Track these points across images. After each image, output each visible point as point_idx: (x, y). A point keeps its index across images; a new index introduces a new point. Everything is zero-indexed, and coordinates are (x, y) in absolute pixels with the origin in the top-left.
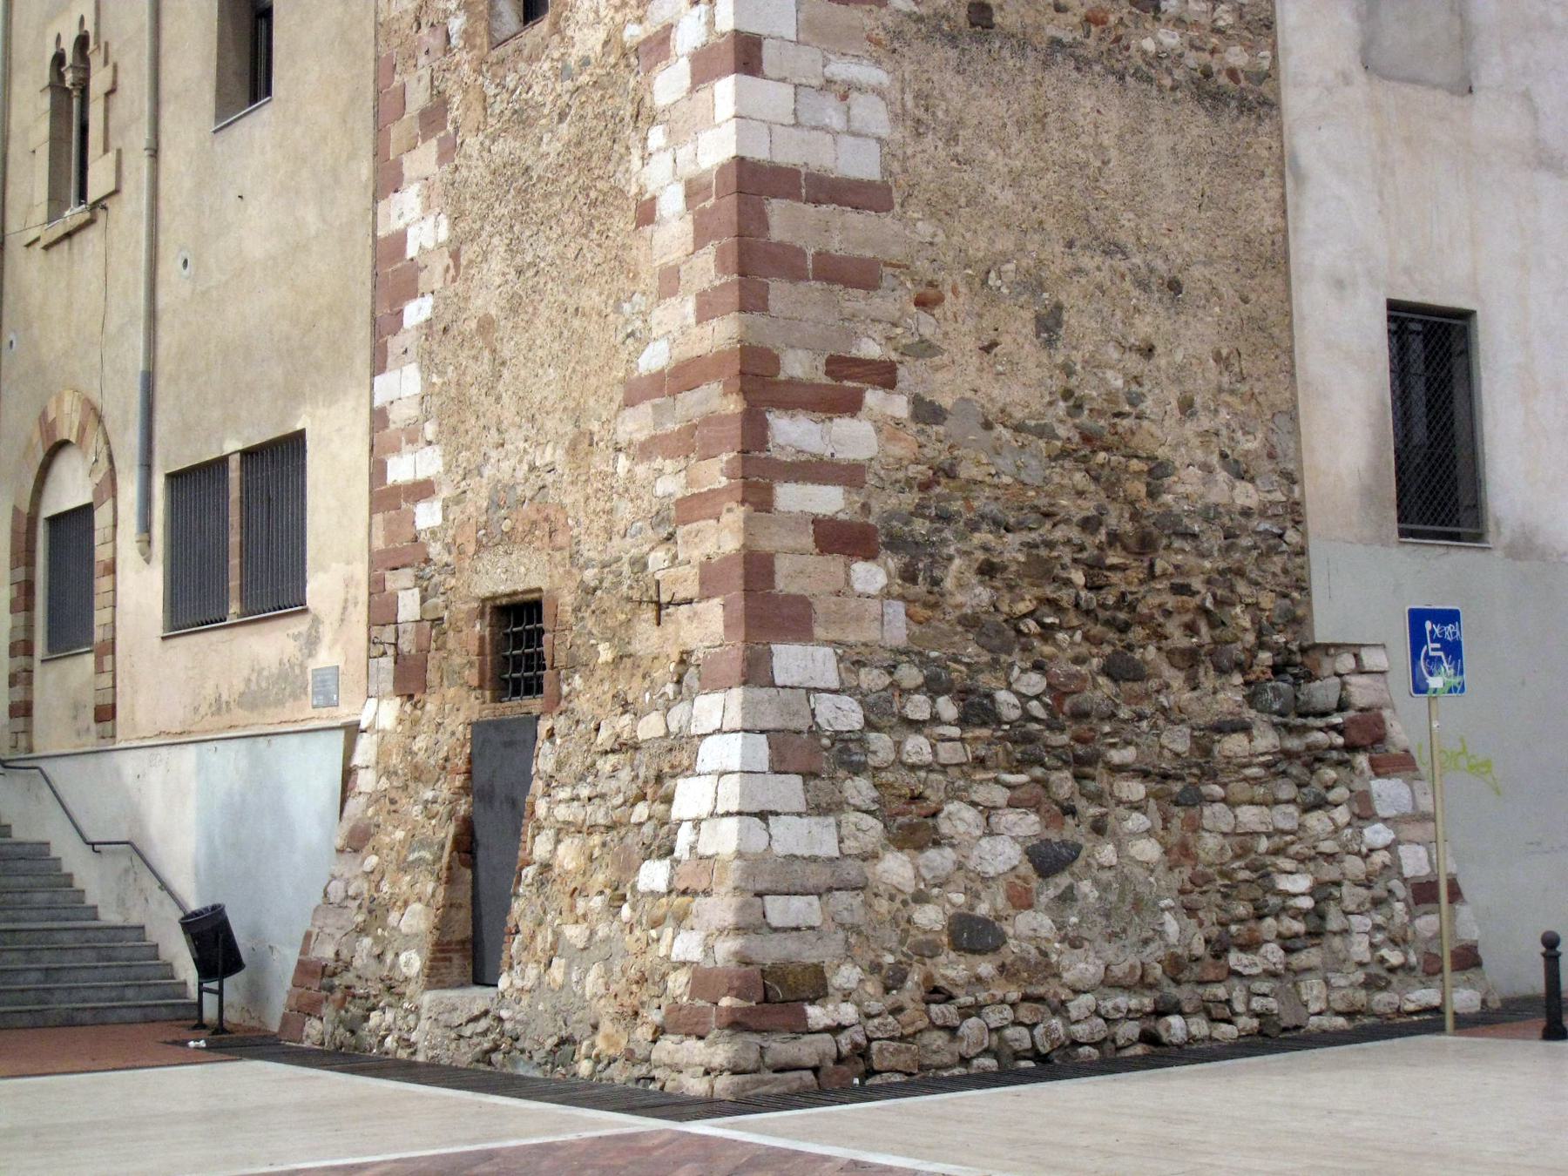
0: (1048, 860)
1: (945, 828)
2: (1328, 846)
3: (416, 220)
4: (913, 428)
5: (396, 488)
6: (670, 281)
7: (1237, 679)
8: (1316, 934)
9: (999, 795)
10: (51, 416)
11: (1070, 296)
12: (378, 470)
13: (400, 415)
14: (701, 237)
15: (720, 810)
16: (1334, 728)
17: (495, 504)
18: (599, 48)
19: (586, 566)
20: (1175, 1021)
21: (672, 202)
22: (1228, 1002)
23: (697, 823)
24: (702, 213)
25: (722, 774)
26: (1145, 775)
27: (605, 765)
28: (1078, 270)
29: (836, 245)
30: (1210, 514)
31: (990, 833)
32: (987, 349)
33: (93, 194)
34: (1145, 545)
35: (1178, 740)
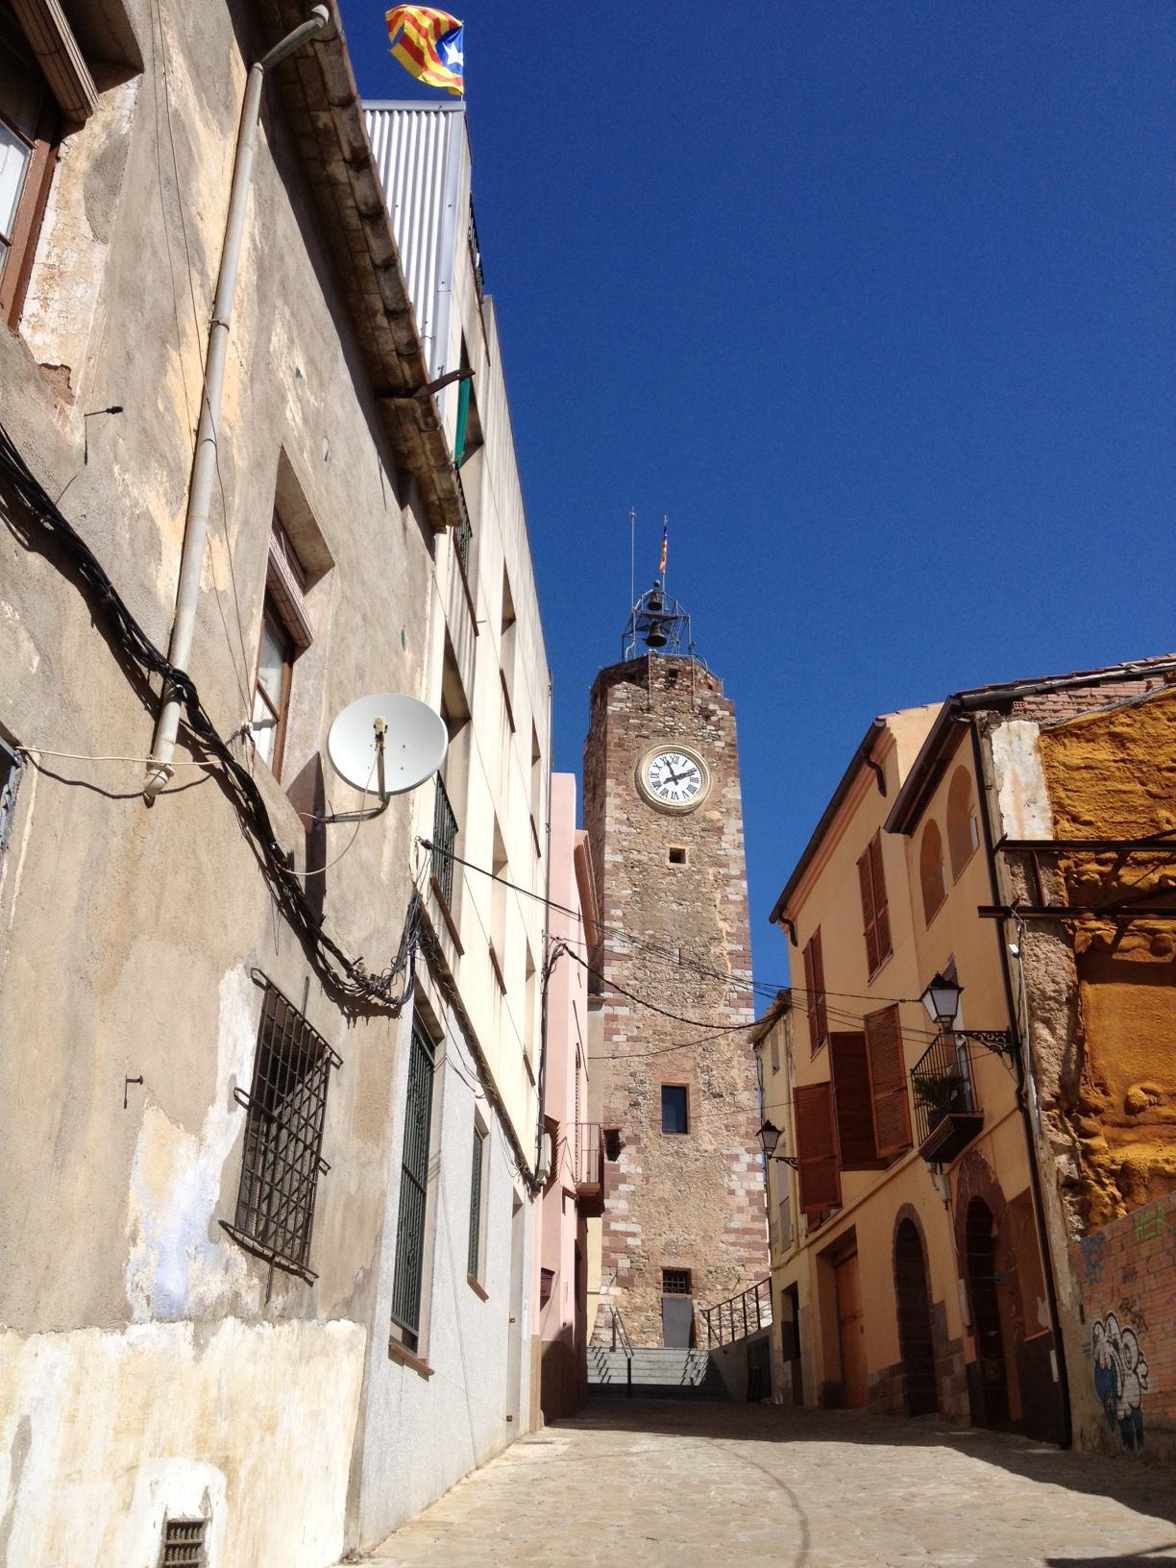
6: (740, 1210)
14: (752, 1203)
21: (741, 1193)
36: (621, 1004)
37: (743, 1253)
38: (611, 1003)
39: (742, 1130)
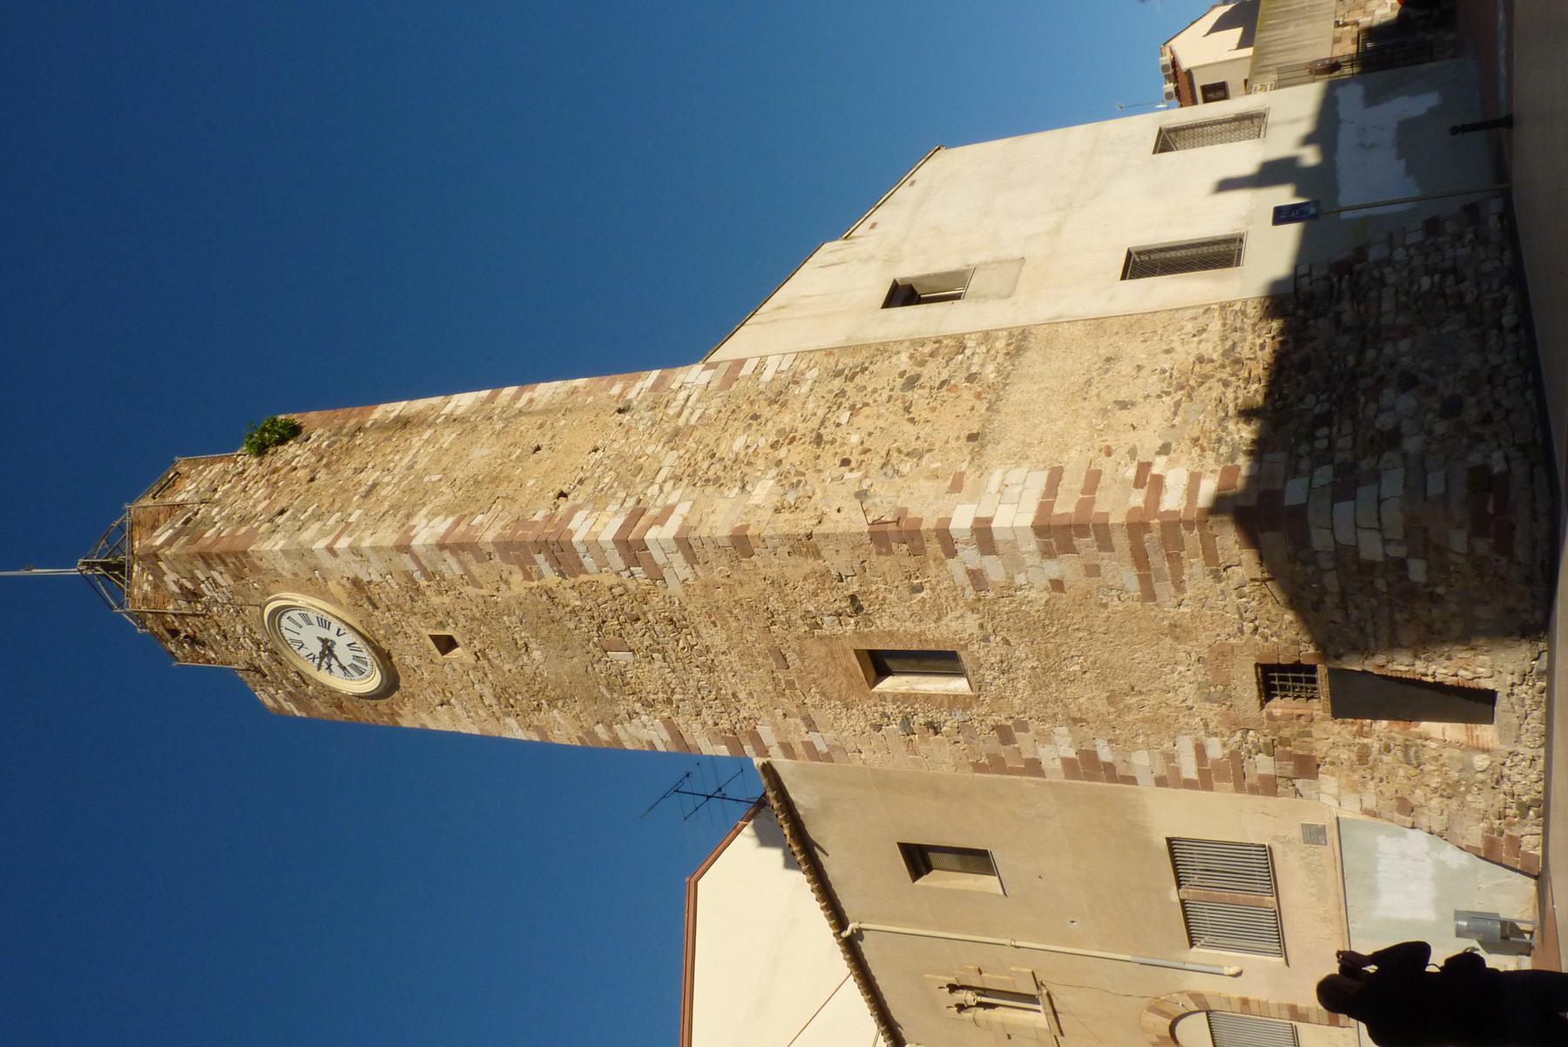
0: (1408, 382)
1: (1390, 427)
2: (1405, 274)
3: (1059, 748)
4: (1172, 455)
5: (1201, 772)
6: (1093, 571)
7: (1312, 322)
8: (1454, 271)
9: (1372, 406)
10: (1156, 1040)
11: (1109, 397)
12: (1189, 784)
13: (1160, 770)
14: (1069, 548)
15: (1375, 525)
16: (1340, 281)
17: (1209, 698)
18: (976, 616)
19: (1241, 631)
20: (1505, 320)
21: (1053, 569)
22: (1494, 300)
23: (1386, 542)
24: (1059, 548)
25: (1356, 526)
26: (1361, 352)
27: (1354, 613)
28: (1098, 395)
29: (1080, 486)
30: (1224, 339)
31: (1393, 408)
32: (1134, 428)
33: (1032, 990)
34: (1238, 361)
35: (1344, 340)
36: (755, 738)
37: (1195, 568)
38: (763, 751)
39: (911, 563)
